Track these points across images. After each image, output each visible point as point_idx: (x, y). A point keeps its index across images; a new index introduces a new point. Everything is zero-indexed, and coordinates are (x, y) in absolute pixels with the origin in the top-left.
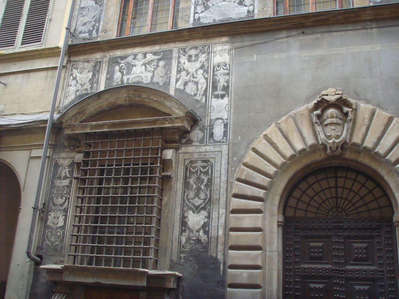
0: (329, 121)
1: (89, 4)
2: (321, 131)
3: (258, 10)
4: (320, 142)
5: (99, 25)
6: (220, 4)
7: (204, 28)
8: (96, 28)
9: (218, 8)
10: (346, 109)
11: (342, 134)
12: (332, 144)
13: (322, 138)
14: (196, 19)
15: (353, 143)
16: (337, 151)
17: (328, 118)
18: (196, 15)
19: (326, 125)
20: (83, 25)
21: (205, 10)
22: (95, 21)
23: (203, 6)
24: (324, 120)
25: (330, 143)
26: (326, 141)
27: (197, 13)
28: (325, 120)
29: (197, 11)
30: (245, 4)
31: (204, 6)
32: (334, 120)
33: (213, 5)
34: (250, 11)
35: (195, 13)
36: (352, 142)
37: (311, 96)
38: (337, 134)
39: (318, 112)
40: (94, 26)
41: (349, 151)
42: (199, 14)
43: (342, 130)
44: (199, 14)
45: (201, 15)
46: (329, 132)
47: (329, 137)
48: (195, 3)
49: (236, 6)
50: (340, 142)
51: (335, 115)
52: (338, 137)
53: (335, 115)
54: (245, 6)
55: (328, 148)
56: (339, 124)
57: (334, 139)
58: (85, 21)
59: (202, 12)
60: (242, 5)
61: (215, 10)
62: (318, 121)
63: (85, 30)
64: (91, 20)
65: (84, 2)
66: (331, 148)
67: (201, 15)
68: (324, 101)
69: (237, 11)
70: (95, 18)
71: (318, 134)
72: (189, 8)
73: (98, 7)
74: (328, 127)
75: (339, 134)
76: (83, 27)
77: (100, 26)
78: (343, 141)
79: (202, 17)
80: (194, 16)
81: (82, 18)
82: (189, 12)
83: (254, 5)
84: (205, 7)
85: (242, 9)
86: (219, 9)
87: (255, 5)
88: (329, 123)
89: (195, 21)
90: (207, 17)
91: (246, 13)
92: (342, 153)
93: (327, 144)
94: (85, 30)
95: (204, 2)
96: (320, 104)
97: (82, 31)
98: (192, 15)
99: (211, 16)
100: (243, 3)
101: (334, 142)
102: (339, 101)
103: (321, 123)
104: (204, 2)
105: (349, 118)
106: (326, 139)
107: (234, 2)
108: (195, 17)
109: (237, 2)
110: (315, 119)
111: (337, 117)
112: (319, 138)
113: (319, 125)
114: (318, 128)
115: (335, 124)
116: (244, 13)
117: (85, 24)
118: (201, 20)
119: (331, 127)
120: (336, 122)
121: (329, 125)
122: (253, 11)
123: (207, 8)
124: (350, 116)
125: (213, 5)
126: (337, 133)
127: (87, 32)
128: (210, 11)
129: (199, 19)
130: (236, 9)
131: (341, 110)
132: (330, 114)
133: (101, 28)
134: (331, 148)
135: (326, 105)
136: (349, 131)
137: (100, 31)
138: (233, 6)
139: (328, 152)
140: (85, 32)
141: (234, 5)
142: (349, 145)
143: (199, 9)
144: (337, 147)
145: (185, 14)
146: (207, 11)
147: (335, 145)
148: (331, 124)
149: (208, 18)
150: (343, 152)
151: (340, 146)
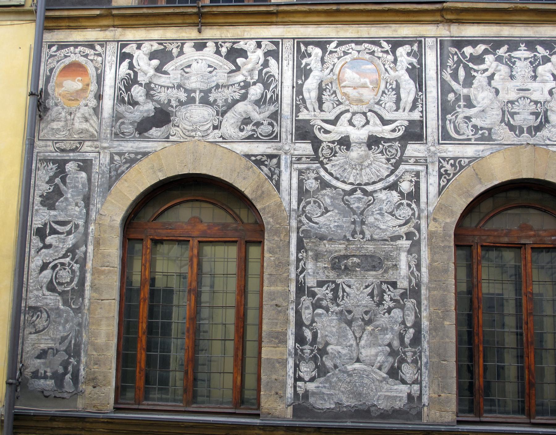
1: (49, 301)
3: (430, 398)
5: (79, 362)
6: (349, 368)
7: (323, 430)
8: (70, 368)
9: (345, 375)
14: (298, 394)
18: (299, 383)
20: (39, 357)
21: (319, 376)
22: (67, 351)
23: (312, 365)
27: (300, 379)
29: (301, 374)
30: (404, 377)
31: (316, 364)
33: (336, 367)
34: (413, 397)
35: (298, 379)
40: (65, 364)
42: (305, 382)
44: (305, 382)
45: (311, 386)
48: (296, 354)
49: (384, 379)
54: (404, 382)
58: (43, 346)
59: (312, 380)
60: (397, 379)
61: (340, 380)
63: (45, 372)
64: (58, 345)
65: (35, 292)
67: (311, 386)
69: (387, 391)
70: (67, 342)
72: (284, 363)
73: (72, 314)
76: (39, 361)
77: (82, 367)
79: (314, 393)
80: (295, 387)
81: (33, 336)
82: (283, 373)
83: (421, 384)
84: (317, 367)
85: (396, 387)
86: (348, 380)
87: (424, 384)
89: (299, 400)
90: (323, 393)
91: (405, 400)
94: (45, 372)
95: (315, 355)
97: (37, 371)
98: (290, 381)
99: (332, 395)
100: (398, 373)
104: (315, 355)
107: (380, 368)
108: (298, 389)
109: (386, 370)
116: (401, 399)
117: (43, 354)
118: (312, 400)
122: (420, 397)
123: (322, 371)
125: (336, 367)
127: (51, 378)
128: (326, 381)
129: (306, 395)
130: (385, 386)
133: (82, 373)
137: (81, 379)
138: (378, 378)
140: (45, 377)
141: (381, 376)
143: (306, 370)
145: (274, 377)
146: (322, 379)
149: (326, 398)
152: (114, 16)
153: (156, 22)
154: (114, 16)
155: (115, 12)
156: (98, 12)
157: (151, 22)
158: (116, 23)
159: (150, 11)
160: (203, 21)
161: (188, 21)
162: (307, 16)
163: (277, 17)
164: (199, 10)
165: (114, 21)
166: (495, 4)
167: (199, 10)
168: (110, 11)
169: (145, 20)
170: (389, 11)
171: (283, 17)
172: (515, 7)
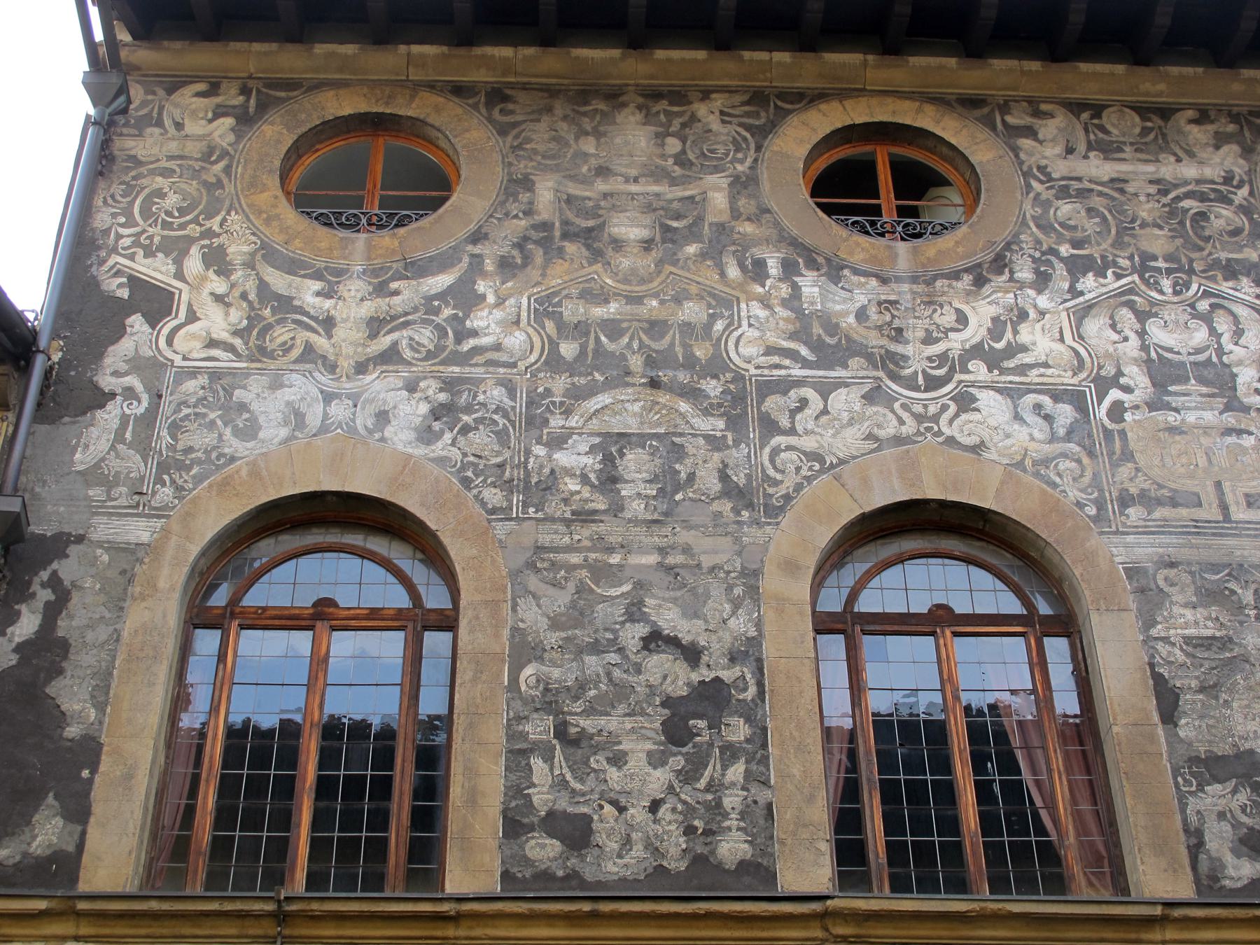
152: (79, 915)
153: (177, 931)
154: (79, 915)
155: (82, 905)
156: (42, 905)
157: (165, 931)
158: (84, 931)
159: (166, 906)
160: (287, 932)
161: (251, 932)
162: (525, 927)
163: (457, 927)
164: (280, 907)
165: (78, 927)
166: (939, 903)
167: (280, 907)
168: (70, 903)
169: (150, 927)
170: (709, 916)
171: (471, 928)
172: (982, 909)
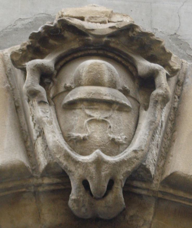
0: (81, 92)
2: (51, 123)
4: (43, 162)
10: (144, 65)
11: (129, 142)
12: (92, 169)
13: (51, 144)
15: (172, 174)
16: (110, 197)
17: (79, 85)
19: (72, 105)
24: (62, 89)
25: (85, 165)
26: (67, 156)
28: (68, 89)
32: (105, 92)
36: (168, 173)
37: (17, 30)
38: (112, 136)
39: (48, 61)
41: (152, 210)
43: (132, 126)
46: (82, 128)
47: (79, 144)
50: (122, 163)
51: (106, 78)
52: (114, 146)
53: (106, 78)
55: (74, 184)
56: (122, 108)
57: (98, 151)
62: (39, 87)
66: (85, 184)
68: (67, 34)
71: (35, 134)
74: (78, 111)
75: (121, 137)
78: (137, 162)
88: (82, 100)
92: (123, 213)
93: (72, 168)
96: (51, 41)
101: (99, 162)
102: (123, 39)
103: (53, 100)
105: (158, 91)
106: (66, 148)
110: (30, 82)
111: (113, 85)
112: (39, 148)
113: (41, 102)
114: (41, 113)
115: (104, 107)
119: (88, 112)
120: (108, 98)
121: (82, 106)
124: (164, 85)
126: (111, 132)
131: (128, 67)
132: (89, 72)
134: (85, 184)
135: (75, 45)
136: (158, 138)
139: (73, 196)
142: (156, 185)
144: (111, 183)
147: (105, 172)
148: (92, 102)
150: (131, 212)
151: (121, 177)
